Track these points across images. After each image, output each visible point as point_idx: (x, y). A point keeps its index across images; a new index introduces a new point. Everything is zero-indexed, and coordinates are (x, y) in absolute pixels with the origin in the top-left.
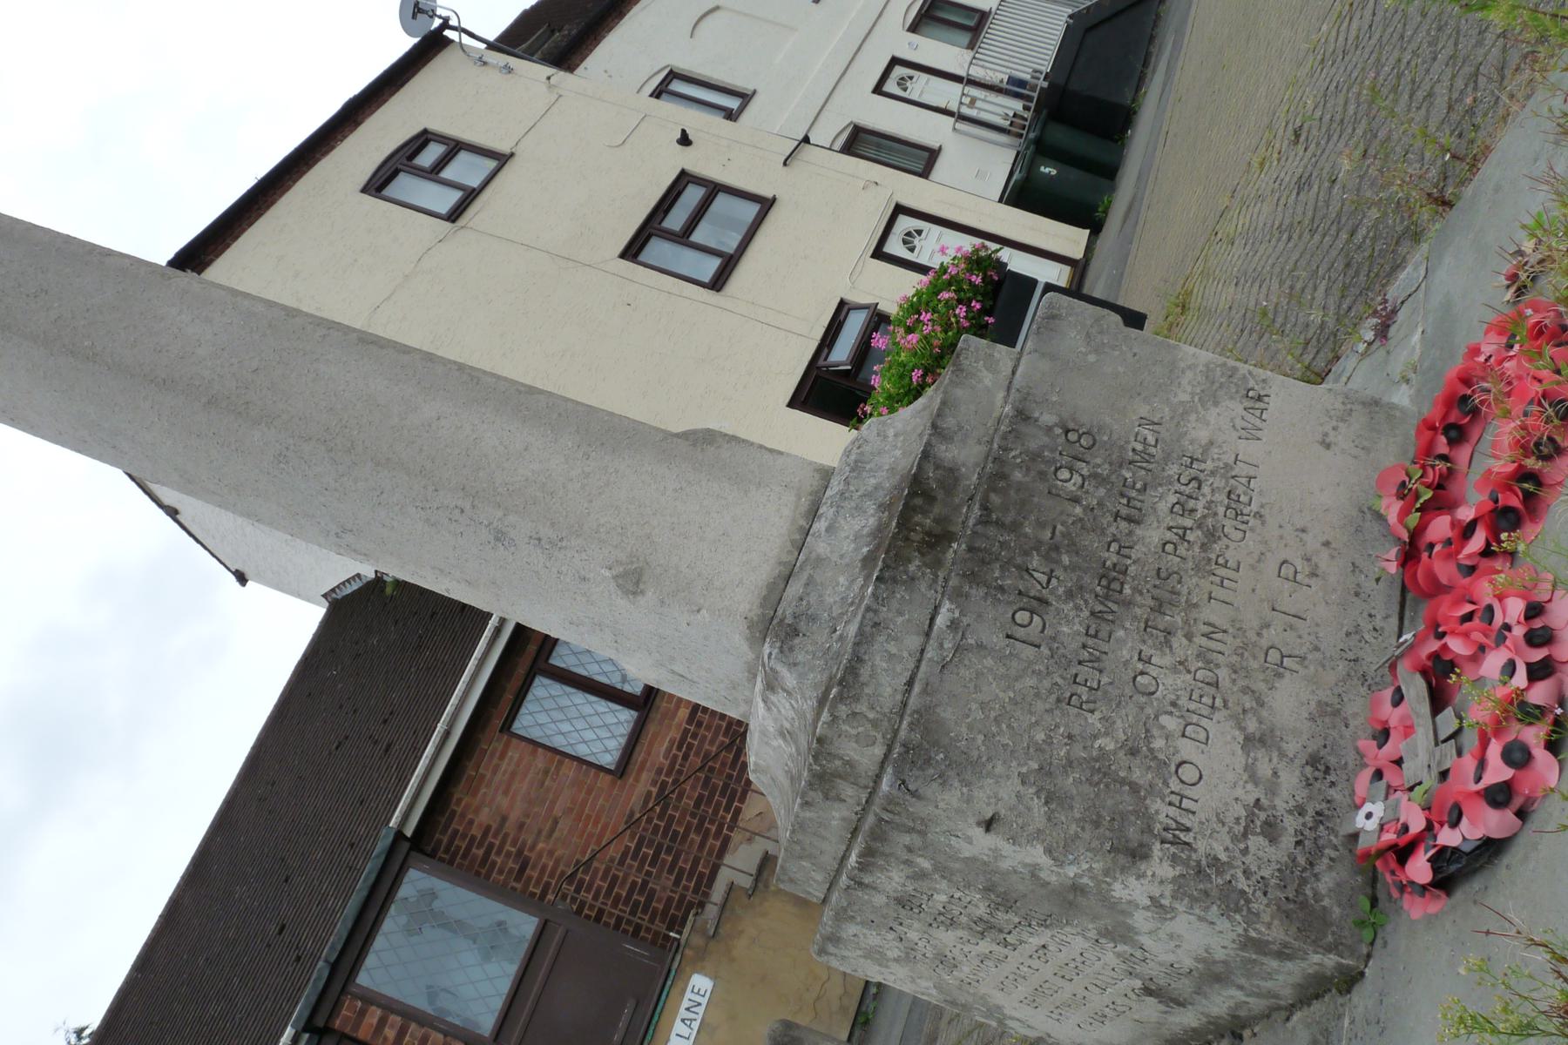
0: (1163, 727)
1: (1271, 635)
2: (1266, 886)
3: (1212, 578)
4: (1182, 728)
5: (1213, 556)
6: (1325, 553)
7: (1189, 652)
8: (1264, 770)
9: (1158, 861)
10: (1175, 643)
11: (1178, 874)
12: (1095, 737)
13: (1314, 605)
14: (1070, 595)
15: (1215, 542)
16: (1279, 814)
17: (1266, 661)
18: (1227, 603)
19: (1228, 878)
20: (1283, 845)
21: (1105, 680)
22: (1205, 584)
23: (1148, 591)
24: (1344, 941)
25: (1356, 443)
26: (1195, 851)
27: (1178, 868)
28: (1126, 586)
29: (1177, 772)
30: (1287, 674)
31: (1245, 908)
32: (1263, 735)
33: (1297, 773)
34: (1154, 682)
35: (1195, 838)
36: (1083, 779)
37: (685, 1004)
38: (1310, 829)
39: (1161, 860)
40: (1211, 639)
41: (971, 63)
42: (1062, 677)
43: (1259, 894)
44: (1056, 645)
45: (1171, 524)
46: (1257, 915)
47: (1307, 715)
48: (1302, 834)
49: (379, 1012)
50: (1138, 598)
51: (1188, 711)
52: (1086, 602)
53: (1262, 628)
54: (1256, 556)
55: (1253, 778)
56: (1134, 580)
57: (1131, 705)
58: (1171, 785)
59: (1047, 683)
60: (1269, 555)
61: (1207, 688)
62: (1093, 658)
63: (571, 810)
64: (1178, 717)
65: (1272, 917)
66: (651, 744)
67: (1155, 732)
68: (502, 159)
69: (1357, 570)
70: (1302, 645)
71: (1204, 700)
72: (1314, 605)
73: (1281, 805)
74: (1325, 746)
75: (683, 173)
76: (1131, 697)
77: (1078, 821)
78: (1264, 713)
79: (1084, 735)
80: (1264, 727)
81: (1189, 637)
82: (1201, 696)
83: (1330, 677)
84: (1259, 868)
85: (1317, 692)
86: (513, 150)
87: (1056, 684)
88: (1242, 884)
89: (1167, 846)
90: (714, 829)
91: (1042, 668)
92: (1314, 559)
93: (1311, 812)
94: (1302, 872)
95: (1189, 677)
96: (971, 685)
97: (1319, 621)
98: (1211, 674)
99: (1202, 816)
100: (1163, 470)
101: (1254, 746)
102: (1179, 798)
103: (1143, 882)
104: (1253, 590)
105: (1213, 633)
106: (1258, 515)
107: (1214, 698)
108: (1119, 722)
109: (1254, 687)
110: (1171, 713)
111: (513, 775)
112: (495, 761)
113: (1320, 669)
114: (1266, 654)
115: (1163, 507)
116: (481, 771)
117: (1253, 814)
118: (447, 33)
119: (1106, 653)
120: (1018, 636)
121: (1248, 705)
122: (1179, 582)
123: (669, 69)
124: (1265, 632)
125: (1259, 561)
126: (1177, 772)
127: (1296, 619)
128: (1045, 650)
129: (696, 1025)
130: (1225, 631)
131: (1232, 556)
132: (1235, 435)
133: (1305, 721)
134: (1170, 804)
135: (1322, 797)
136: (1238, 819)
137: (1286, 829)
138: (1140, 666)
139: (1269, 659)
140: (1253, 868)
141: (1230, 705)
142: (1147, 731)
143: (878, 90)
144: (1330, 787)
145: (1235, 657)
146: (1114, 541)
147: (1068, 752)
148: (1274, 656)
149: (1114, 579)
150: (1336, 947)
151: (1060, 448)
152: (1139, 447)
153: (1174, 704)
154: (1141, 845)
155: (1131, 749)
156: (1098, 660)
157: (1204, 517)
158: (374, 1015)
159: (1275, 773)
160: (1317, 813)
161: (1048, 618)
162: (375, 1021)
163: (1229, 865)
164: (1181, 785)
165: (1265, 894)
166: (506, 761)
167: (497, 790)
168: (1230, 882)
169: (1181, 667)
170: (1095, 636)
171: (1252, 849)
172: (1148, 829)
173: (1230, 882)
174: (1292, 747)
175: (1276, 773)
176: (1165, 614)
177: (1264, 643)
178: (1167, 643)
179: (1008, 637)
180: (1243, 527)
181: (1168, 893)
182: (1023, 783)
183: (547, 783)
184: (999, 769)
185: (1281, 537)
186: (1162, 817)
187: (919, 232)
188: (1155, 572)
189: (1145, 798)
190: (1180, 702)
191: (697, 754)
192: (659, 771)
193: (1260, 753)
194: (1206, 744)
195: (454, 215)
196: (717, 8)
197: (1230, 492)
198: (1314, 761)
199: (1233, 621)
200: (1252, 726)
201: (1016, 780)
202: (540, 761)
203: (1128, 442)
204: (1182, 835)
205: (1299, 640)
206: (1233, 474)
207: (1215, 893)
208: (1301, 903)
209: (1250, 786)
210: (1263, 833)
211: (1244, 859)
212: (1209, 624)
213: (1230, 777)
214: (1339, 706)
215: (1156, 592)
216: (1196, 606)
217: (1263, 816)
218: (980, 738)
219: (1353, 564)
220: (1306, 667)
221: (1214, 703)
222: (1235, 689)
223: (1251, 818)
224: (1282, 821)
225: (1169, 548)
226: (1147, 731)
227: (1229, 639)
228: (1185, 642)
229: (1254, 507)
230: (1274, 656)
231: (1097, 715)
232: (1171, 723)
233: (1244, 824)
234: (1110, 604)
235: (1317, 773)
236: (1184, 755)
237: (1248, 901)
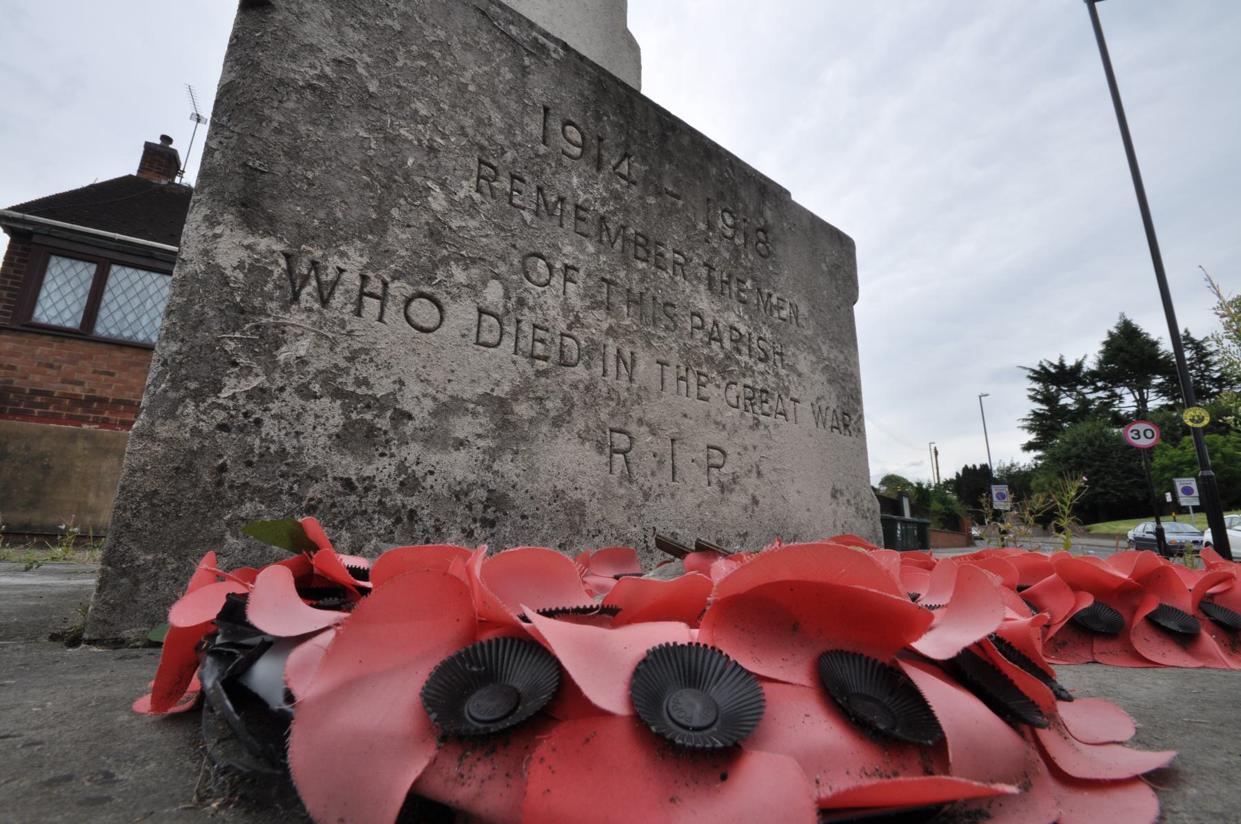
0: (485, 284)
1: (644, 438)
2: (241, 429)
3: (683, 368)
4: (492, 309)
5: (704, 370)
6: (746, 500)
7: (594, 331)
8: (462, 427)
9: (246, 242)
10: (600, 314)
11: (228, 272)
12: (443, 185)
13: (692, 491)
14: (616, 196)
15: (719, 373)
16: (394, 450)
17: (612, 430)
18: (662, 383)
19: (243, 360)
20: (336, 458)
21: (528, 216)
22: (674, 358)
23: (647, 289)
24: (144, 587)
25: (846, 526)
26: (285, 308)
27: (241, 276)
28: (644, 265)
29: (422, 295)
30: (605, 459)
31: (182, 392)
32: (515, 427)
33: (472, 477)
34: (542, 280)
35: (310, 310)
36: (371, 153)
38: (380, 502)
39: (248, 247)
40: (618, 362)
42: (514, 161)
43: (221, 416)
44: (553, 164)
45: (720, 325)
46: (171, 414)
47: (560, 487)
48: (367, 490)
50: (636, 276)
51: (518, 322)
52: (614, 213)
53: (649, 425)
54: (719, 419)
55: (448, 408)
56: (654, 274)
57: (503, 245)
58: (397, 284)
59: (500, 138)
60: (725, 434)
61: (555, 349)
62: (550, 207)
64: (505, 306)
65: (167, 441)
67: (475, 272)
69: (742, 539)
70: (645, 476)
71: (538, 344)
72: (692, 491)
73: (412, 451)
74: (524, 517)
76: (514, 246)
77: (292, 126)
78: (545, 429)
79: (442, 171)
80: (527, 425)
81: (611, 332)
82: (542, 341)
83: (619, 518)
84: (279, 417)
85: (595, 500)
87: (504, 152)
88: (233, 386)
89: (283, 262)
91: (519, 138)
92: (737, 488)
93: (413, 502)
94: (290, 492)
95: (563, 326)
96: (468, 40)
97: (678, 497)
98: (575, 356)
99: (356, 325)
100: (764, 323)
101: (495, 412)
102: (379, 292)
103: (203, 227)
104: (685, 416)
105: (625, 363)
106: (757, 423)
107: (545, 359)
108: (472, 223)
109: (575, 415)
110: (507, 297)
113: (624, 502)
114: (621, 432)
115: (733, 318)
117: (383, 409)
119: (561, 225)
120: (550, 120)
121: (549, 405)
122: (667, 328)
124: (644, 429)
125: (717, 423)
126: (422, 295)
127: (671, 468)
128: (542, 149)
130: (631, 380)
131: (707, 391)
132: (814, 399)
133: (551, 485)
134: (364, 278)
135: (442, 518)
136: (365, 382)
137: (369, 463)
138: (558, 265)
139: (616, 435)
140: (275, 407)
141: (543, 380)
142: (473, 261)
144: (464, 531)
145: (605, 389)
146: (686, 259)
147: (406, 140)
148: (621, 441)
149: (648, 252)
150: (124, 573)
151: (749, 220)
152: (774, 300)
153: (521, 302)
154: (272, 220)
155: (439, 232)
156: (551, 215)
157: (738, 363)
159: (460, 444)
160: (412, 514)
161: (582, 166)
163: (271, 366)
164: (400, 298)
165: (222, 427)
168: (235, 364)
169: (572, 318)
170: (578, 218)
171: (312, 405)
172: (304, 235)
173: (235, 364)
174: (508, 466)
175: (461, 444)
176: (628, 307)
177: (632, 428)
178: (596, 305)
179: (546, 110)
180: (741, 405)
181: (189, 268)
182: (338, 62)
184: (354, 36)
185: (746, 449)
186: (335, 261)
188: (669, 300)
189: (363, 240)
190: (526, 311)
193: (484, 422)
194: (477, 343)
197: (766, 392)
198: (497, 500)
199: (646, 389)
200: (523, 410)
201: (341, 53)
203: (775, 290)
204: (311, 287)
205: (649, 473)
206: (783, 396)
207: (202, 336)
208: (219, 496)
209: (428, 404)
210: (349, 425)
211: (288, 389)
212: (633, 361)
213: (437, 375)
214: (585, 532)
215: (648, 297)
216: (649, 345)
217: (384, 423)
218: (398, 27)
219: (746, 533)
220: (621, 483)
221: (539, 358)
222: (565, 388)
223: (371, 403)
224: (383, 455)
225: (697, 320)
226: (473, 261)
227: (624, 382)
228: (605, 326)
229: (762, 418)
230: (621, 441)
231: (477, 196)
232: (493, 294)
233: (359, 391)
234: (619, 241)
235: (480, 507)
236: (451, 308)
237: (198, 396)
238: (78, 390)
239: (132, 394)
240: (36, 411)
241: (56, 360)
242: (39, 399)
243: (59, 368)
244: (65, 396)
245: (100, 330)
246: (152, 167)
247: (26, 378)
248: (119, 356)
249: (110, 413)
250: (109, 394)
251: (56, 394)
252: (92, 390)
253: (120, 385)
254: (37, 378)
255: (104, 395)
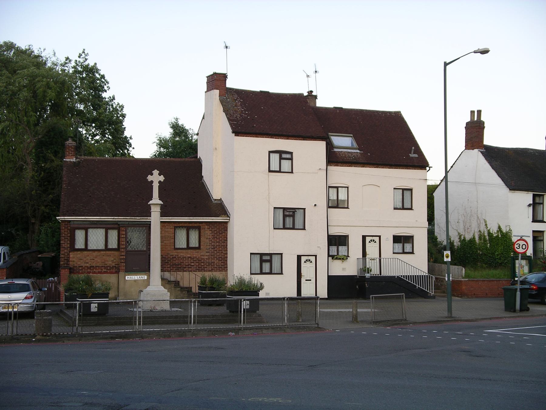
37: (142, 276)
49: (125, 233)
63: (166, 244)
66: (181, 252)
90: (171, 268)
111: (168, 232)
112: (169, 228)
116: (167, 226)
123: (348, 186)
129: (140, 279)
158: (124, 233)
162: (123, 233)
166: (170, 230)
167: (164, 230)
183: (169, 238)
187: (311, 262)
191: (183, 261)
192: (177, 256)
202: (172, 235)
238: (88, 265)
239: (99, 264)
240: (80, 271)
241: (82, 258)
242: (80, 268)
243: (83, 259)
244: (86, 266)
245: (89, 248)
246: (69, 153)
247: (77, 263)
248: (96, 253)
249: (96, 270)
250: (94, 265)
251: (84, 267)
252: (90, 264)
253: (96, 262)
254: (79, 263)
255: (94, 265)
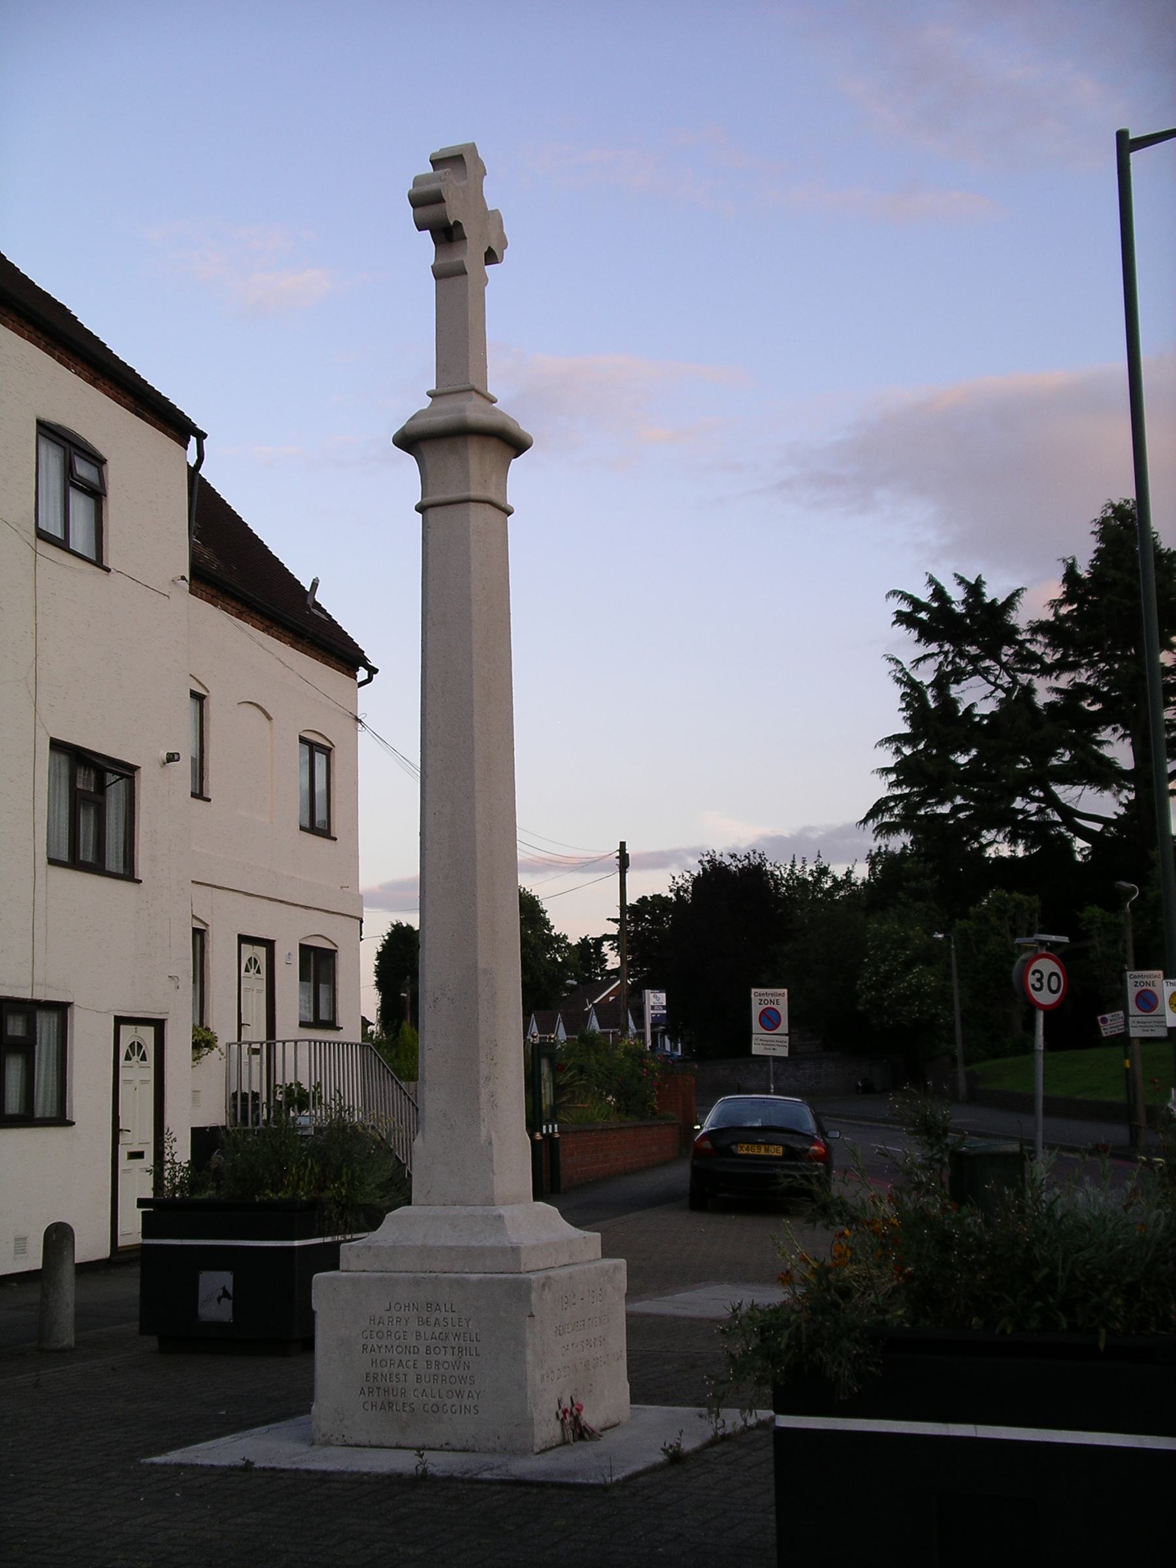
41: (310, 1041)
68: (98, 562)
75: (133, 769)
86: (112, 570)
118: (193, 440)
123: (205, 693)
143: (243, 939)
195: (42, 535)
196: (269, 718)
